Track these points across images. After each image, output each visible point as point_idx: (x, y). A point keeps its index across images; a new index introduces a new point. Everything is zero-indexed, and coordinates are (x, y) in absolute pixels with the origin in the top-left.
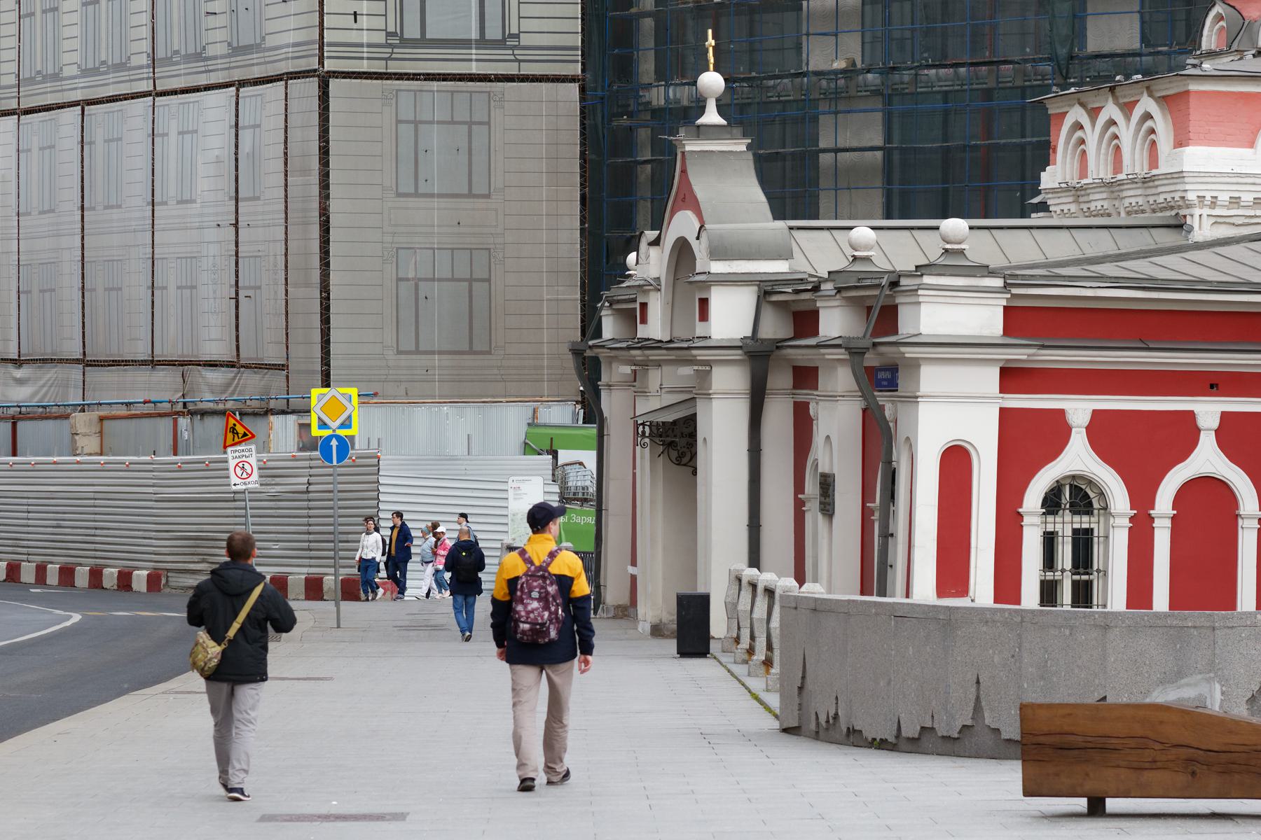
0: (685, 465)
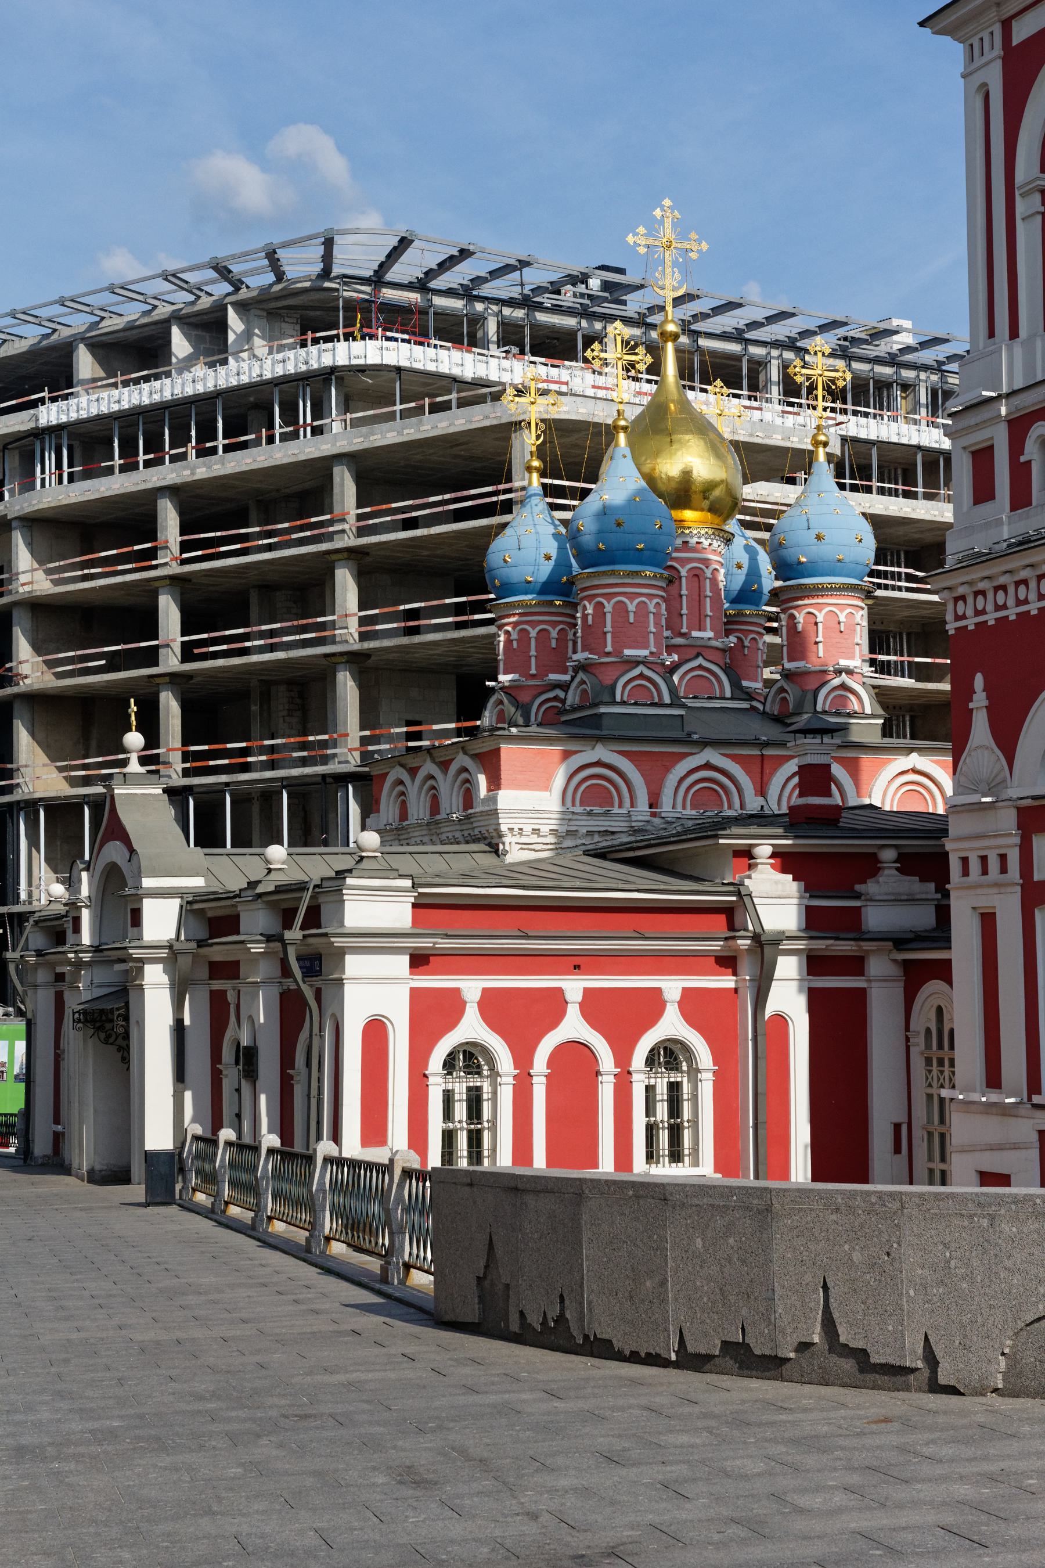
0: (111, 1044)
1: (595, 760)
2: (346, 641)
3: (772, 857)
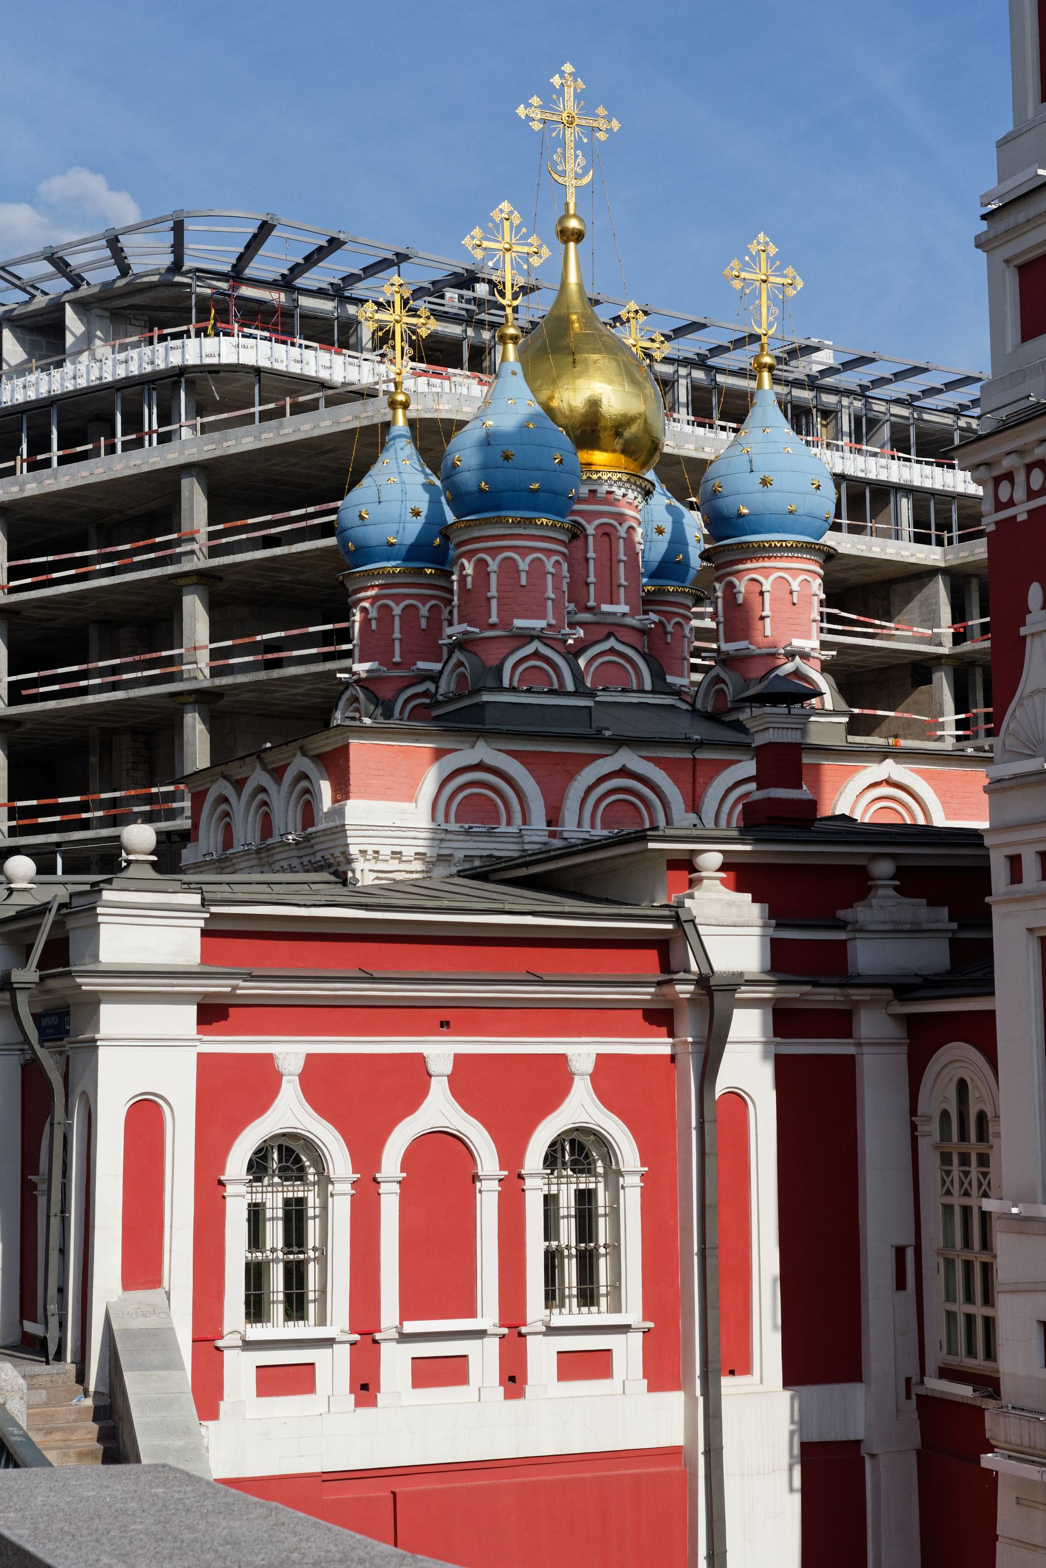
1: (475, 761)
2: (195, 678)
3: (721, 869)
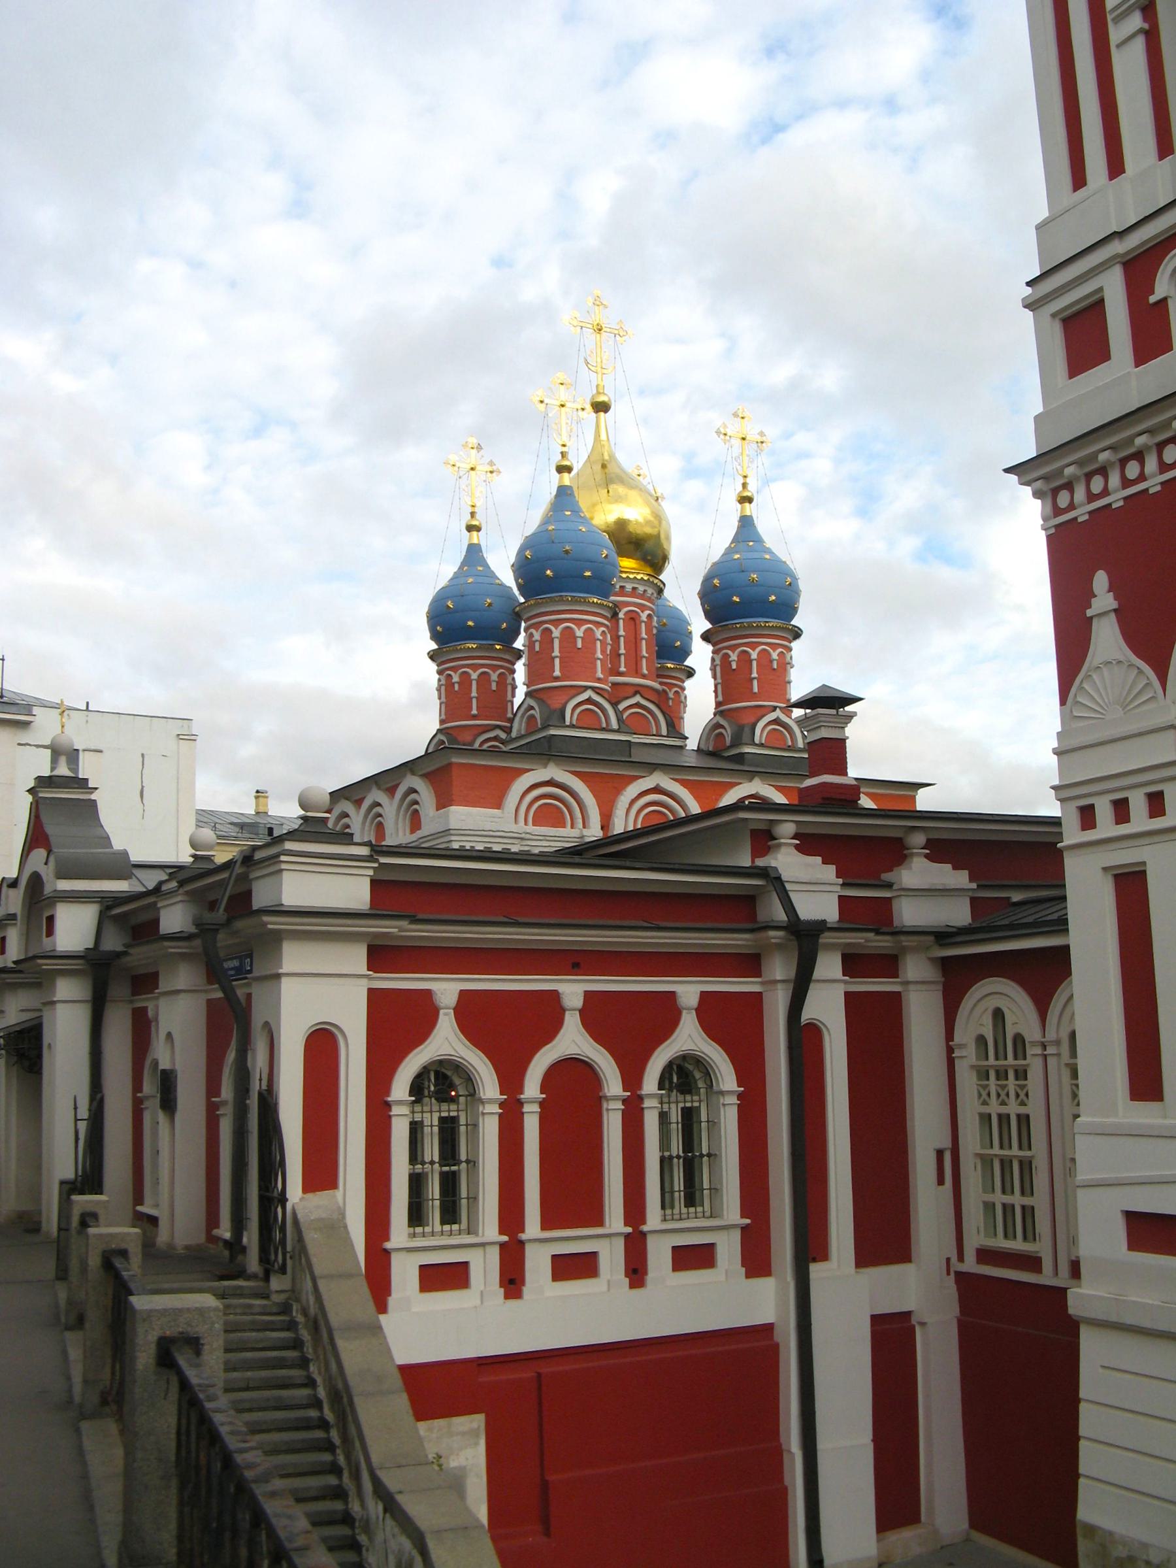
1: (547, 779)
